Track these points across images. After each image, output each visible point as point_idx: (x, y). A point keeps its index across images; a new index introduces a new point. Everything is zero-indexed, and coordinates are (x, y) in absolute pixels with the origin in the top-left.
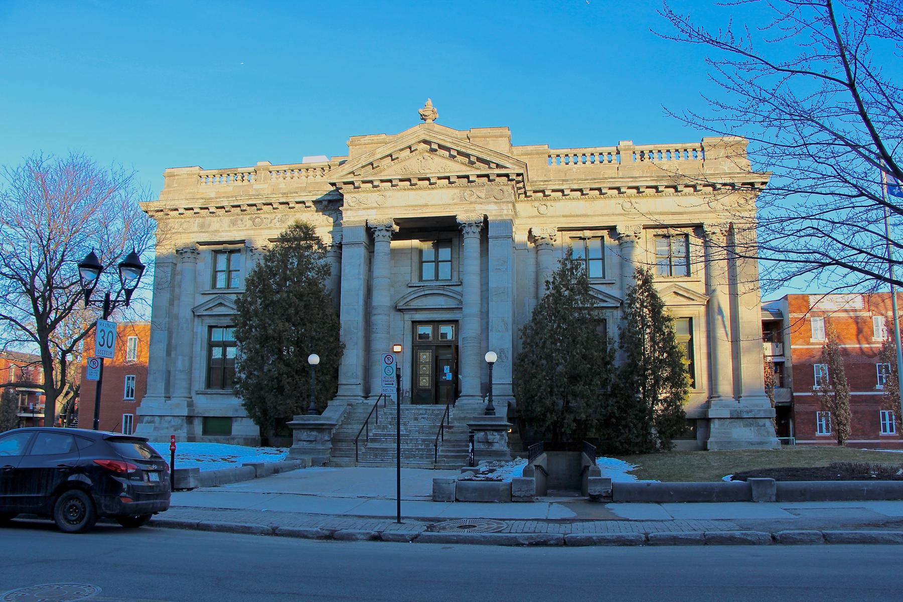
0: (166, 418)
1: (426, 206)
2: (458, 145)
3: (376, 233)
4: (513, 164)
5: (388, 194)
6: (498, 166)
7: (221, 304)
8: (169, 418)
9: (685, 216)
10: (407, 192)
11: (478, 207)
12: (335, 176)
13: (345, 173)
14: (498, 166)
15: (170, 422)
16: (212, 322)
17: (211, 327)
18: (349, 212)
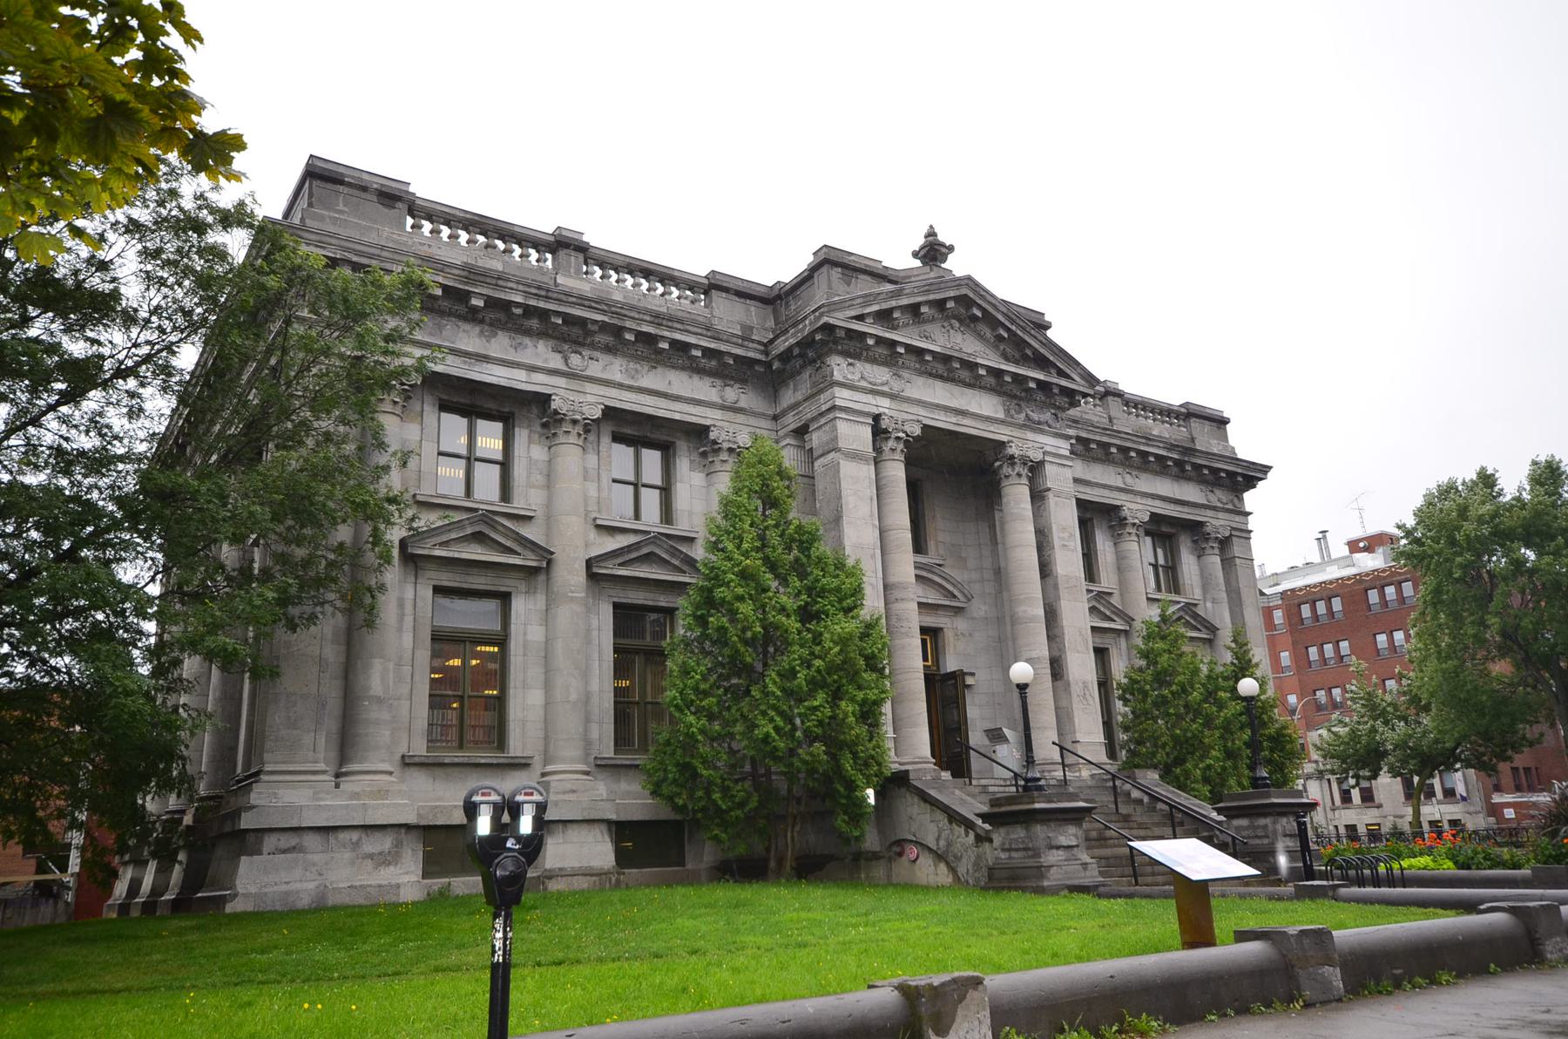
0: (343, 836)
1: (962, 413)
2: (1013, 322)
3: (891, 443)
4: (1082, 377)
5: (905, 374)
6: (1061, 373)
7: (479, 538)
8: (355, 836)
9: (1186, 509)
10: (931, 381)
11: (1030, 435)
12: (837, 315)
13: (853, 313)
14: (1061, 373)
15: (356, 845)
16: (447, 579)
17: (438, 590)
18: (846, 393)
